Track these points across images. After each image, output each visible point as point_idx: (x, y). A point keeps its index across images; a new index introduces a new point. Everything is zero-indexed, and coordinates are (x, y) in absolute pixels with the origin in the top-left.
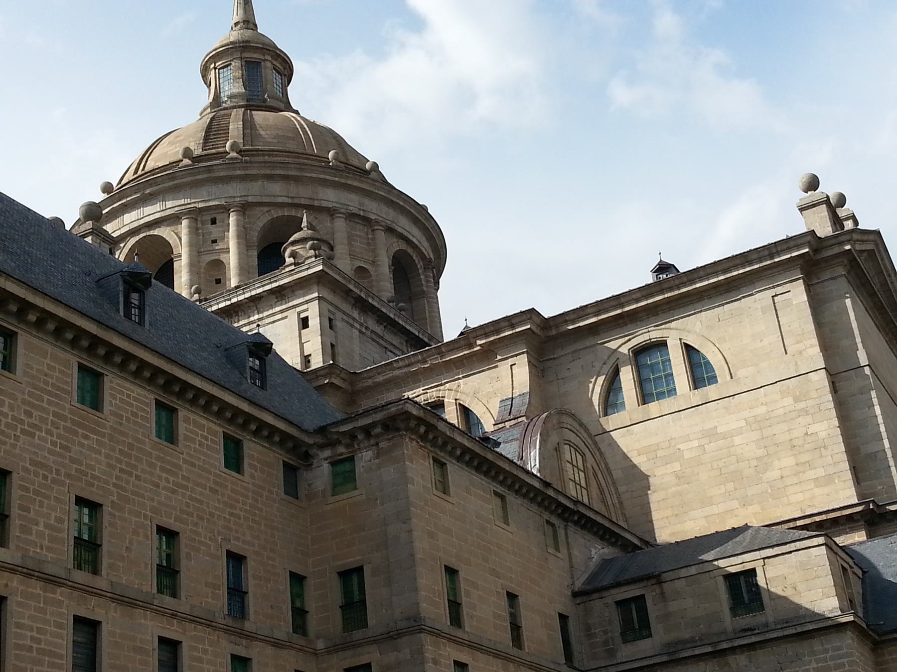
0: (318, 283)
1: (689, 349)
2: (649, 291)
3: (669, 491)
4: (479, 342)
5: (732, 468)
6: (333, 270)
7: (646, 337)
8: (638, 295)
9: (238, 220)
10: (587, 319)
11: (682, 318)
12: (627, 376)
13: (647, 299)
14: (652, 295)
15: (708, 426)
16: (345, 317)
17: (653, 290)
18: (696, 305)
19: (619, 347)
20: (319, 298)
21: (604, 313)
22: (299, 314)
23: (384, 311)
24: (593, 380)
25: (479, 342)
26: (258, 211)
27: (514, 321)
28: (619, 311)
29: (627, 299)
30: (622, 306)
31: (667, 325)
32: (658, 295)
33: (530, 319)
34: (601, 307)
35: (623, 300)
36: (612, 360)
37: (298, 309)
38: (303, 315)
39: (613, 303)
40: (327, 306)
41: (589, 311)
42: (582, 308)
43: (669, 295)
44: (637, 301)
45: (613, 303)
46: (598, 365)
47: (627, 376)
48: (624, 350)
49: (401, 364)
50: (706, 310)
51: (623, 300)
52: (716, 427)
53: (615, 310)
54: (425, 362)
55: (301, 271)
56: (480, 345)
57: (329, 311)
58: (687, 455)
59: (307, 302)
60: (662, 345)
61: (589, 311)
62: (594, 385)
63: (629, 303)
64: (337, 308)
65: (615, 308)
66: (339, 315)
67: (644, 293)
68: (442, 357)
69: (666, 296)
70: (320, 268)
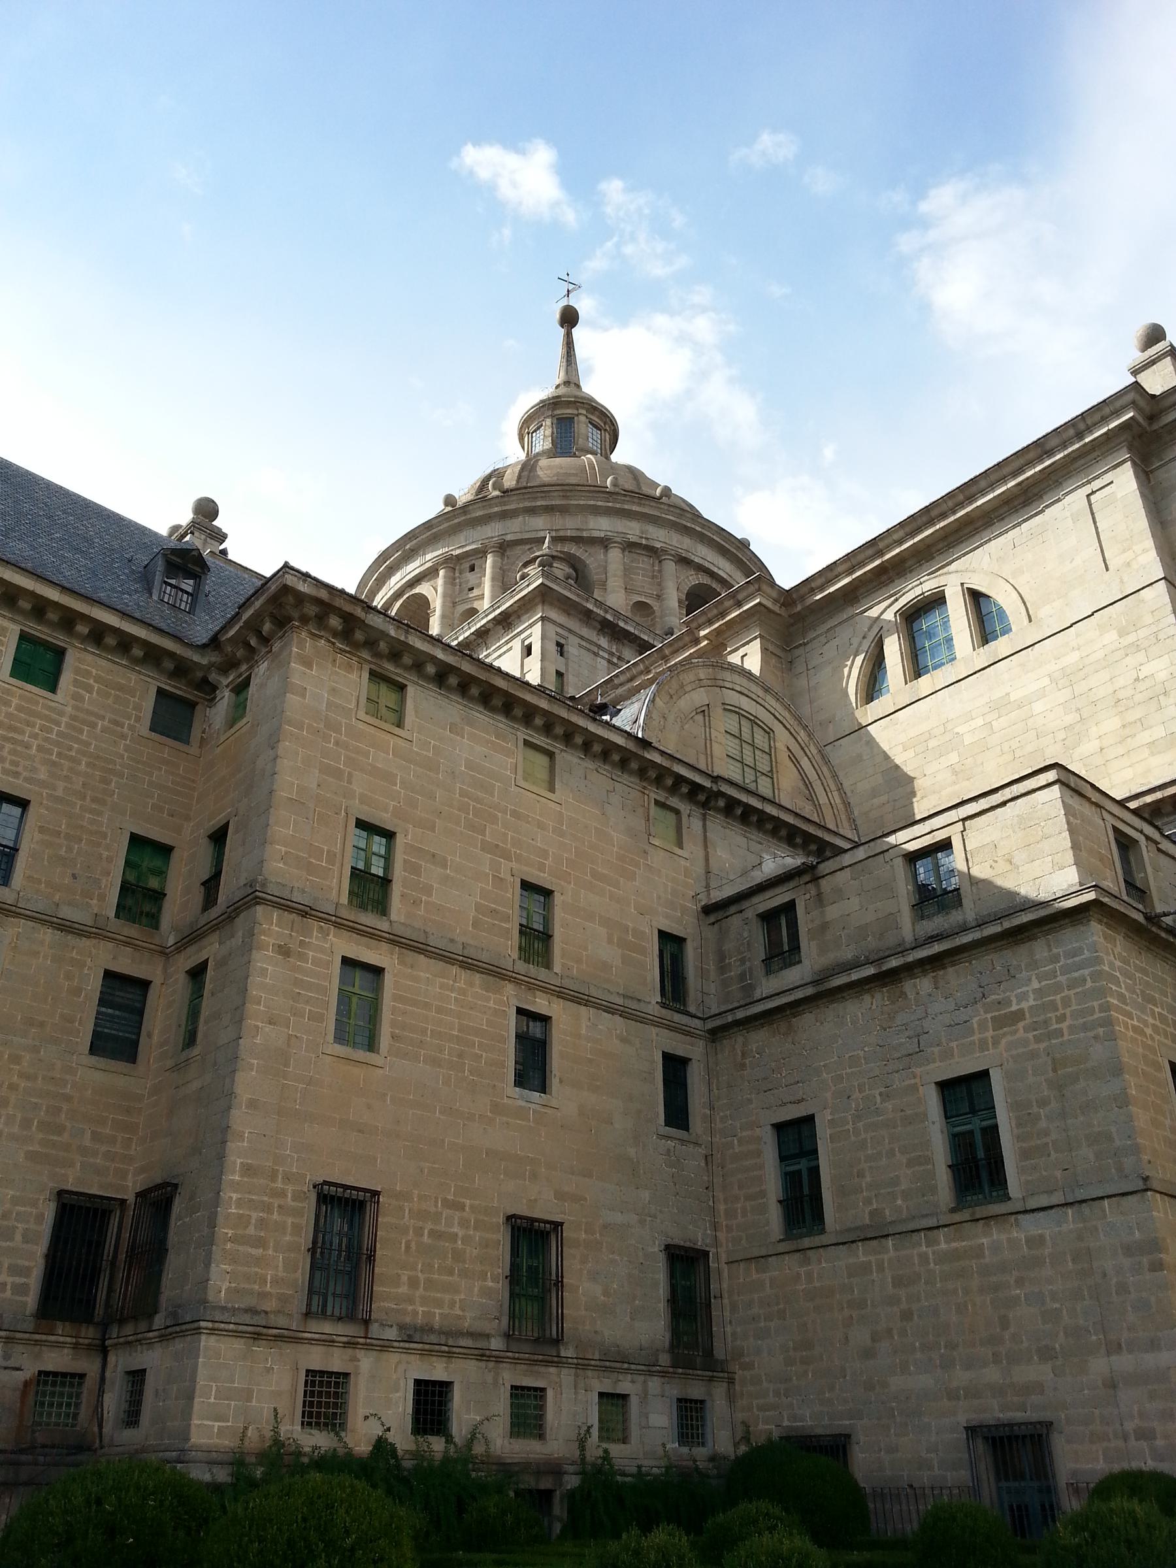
0: (543, 602)
1: (976, 597)
2: (914, 525)
3: (944, 793)
4: (702, 633)
5: (1029, 748)
6: (558, 584)
7: (918, 591)
8: (901, 533)
9: (494, 562)
10: (839, 581)
11: (964, 555)
12: (893, 648)
13: (913, 537)
14: (919, 530)
15: (998, 694)
16: (584, 643)
17: (919, 522)
18: (985, 533)
19: (882, 613)
20: (542, 619)
21: (860, 568)
22: (523, 642)
23: (646, 638)
24: (849, 663)
25: (702, 633)
26: (518, 550)
27: (740, 597)
28: (877, 562)
29: (886, 542)
30: (881, 553)
31: (945, 570)
32: (927, 529)
33: (759, 590)
34: (854, 562)
35: (881, 545)
36: (875, 630)
37: (523, 636)
38: (526, 643)
39: (870, 552)
40: (552, 629)
41: (840, 569)
42: (830, 568)
43: (942, 524)
44: (900, 542)
45: (870, 552)
46: (855, 641)
47: (893, 648)
48: (889, 616)
49: (622, 678)
50: (996, 537)
51: (881, 545)
52: (1008, 694)
53: (872, 561)
54: (649, 672)
55: (521, 590)
56: (705, 637)
57: (557, 634)
58: (968, 740)
59: (531, 626)
60: (937, 600)
61: (840, 569)
62: (851, 668)
63: (889, 548)
64: (570, 631)
65: (872, 558)
66: (574, 640)
67: (907, 529)
68: (666, 662)
69: (938, 527)
70: (540, 581)
